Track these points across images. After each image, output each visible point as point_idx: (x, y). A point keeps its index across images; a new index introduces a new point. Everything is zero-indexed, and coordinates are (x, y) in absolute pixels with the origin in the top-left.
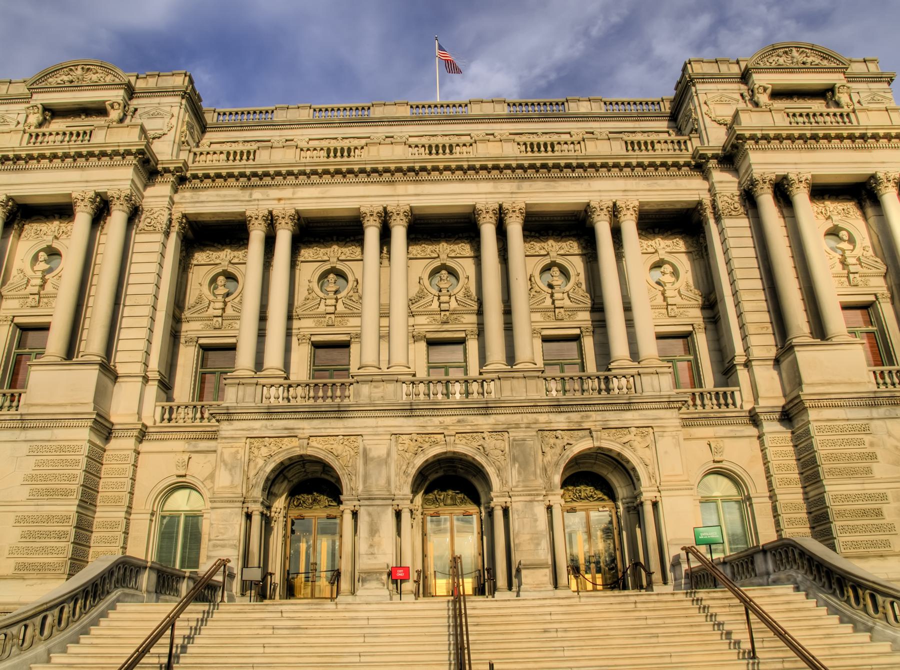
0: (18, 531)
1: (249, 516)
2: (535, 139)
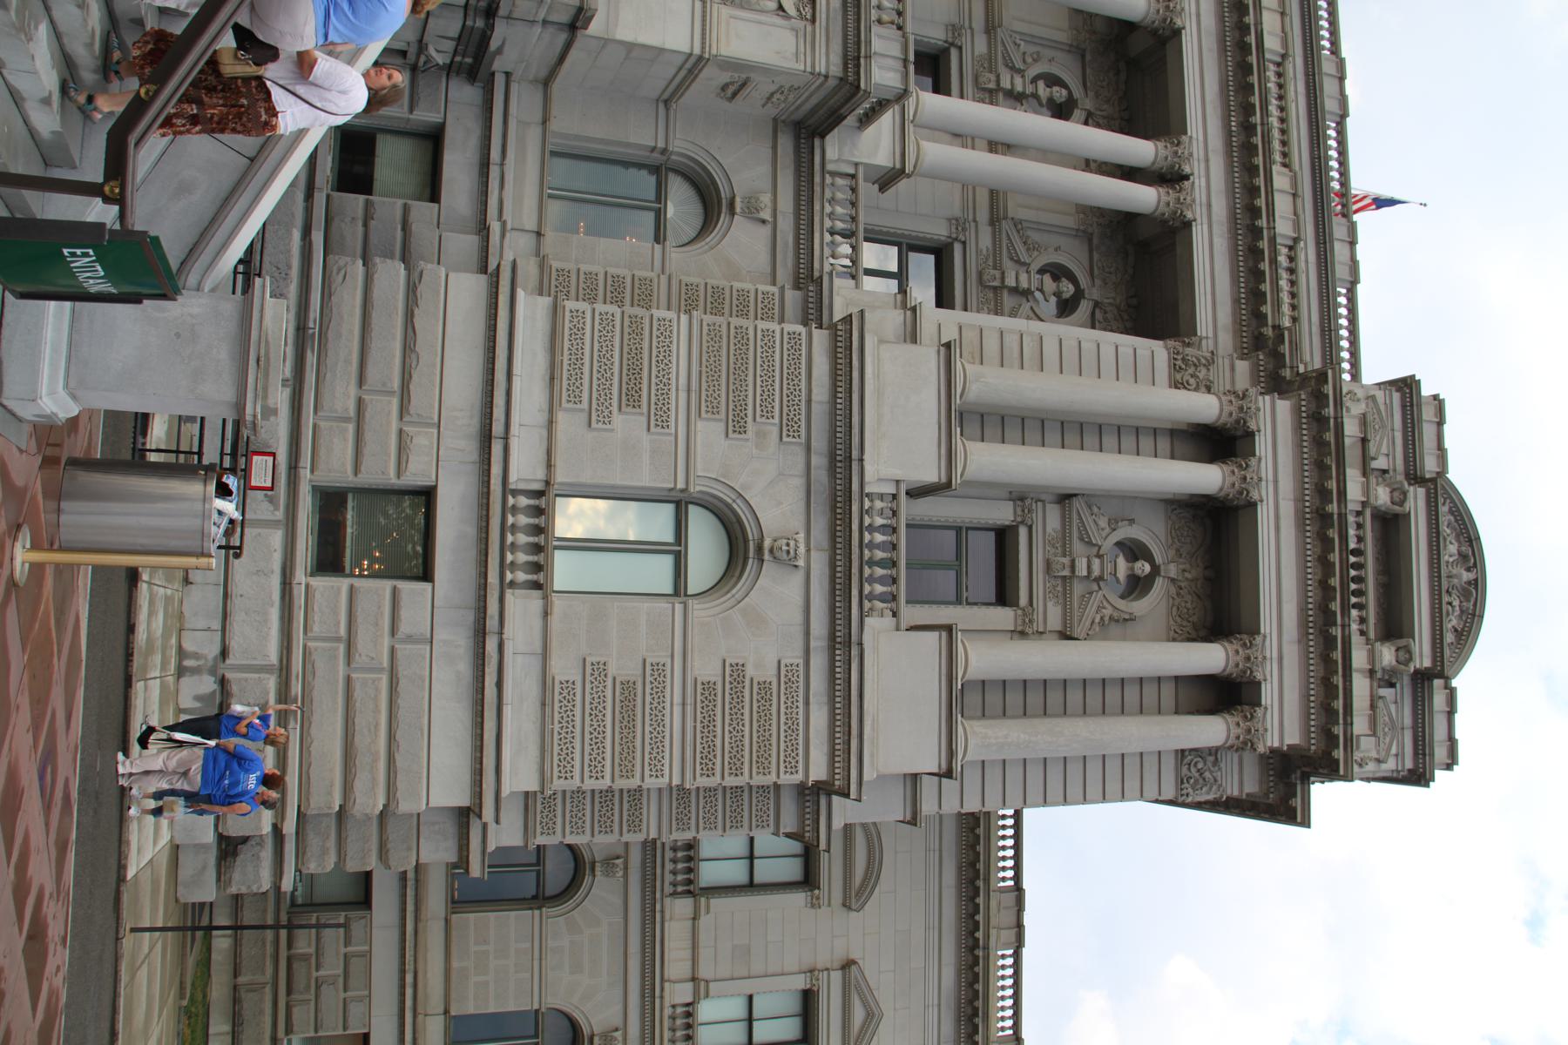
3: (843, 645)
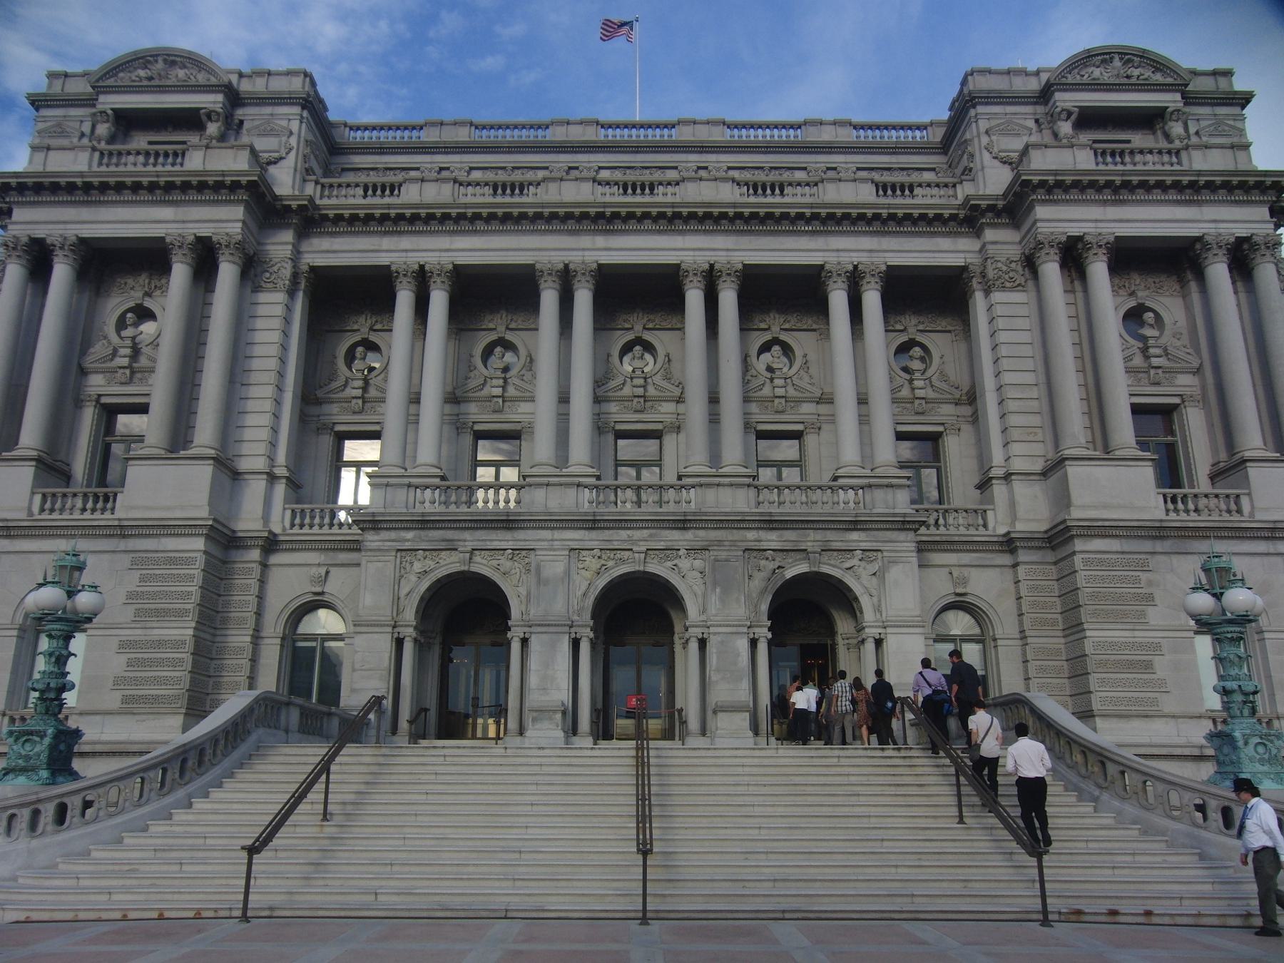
0: (123, 659)
1: (399, 643)
2: (761, 177)
3: (122, 531)
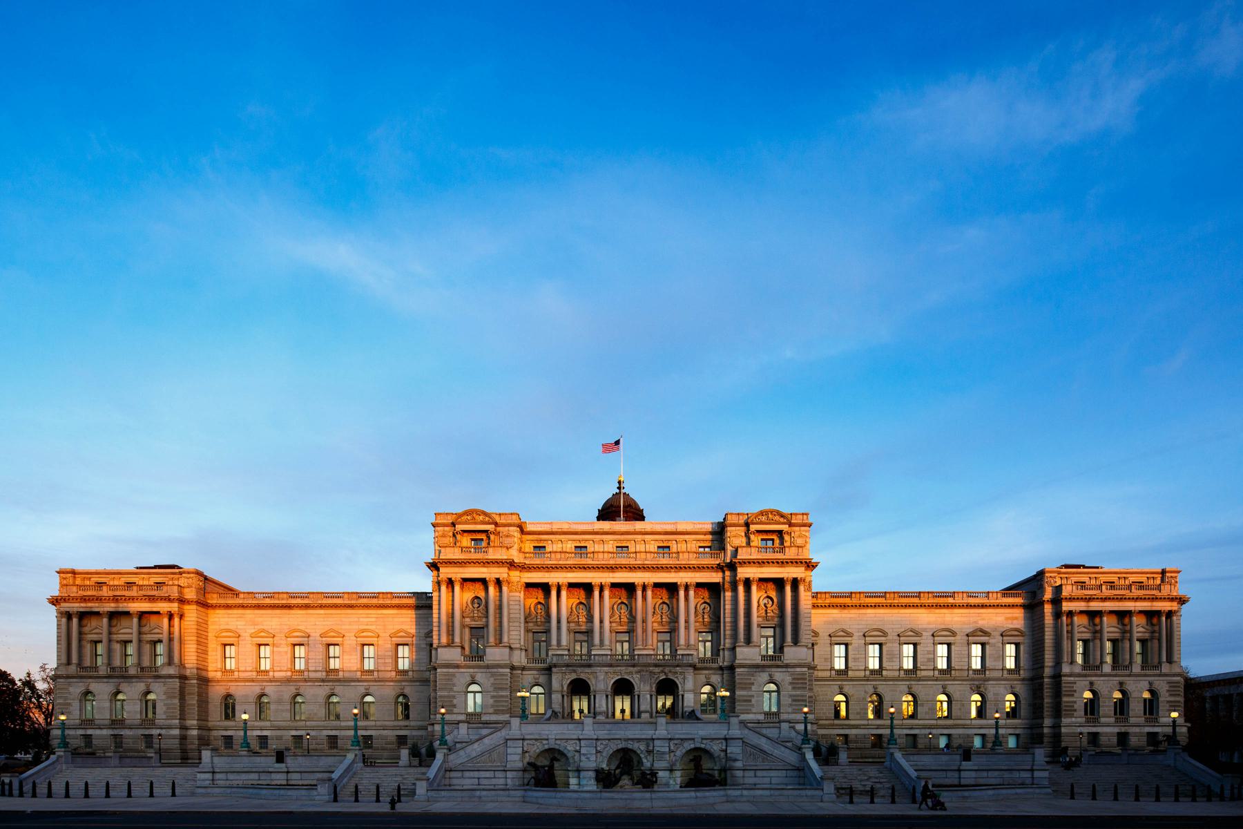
3: (488, 667)
